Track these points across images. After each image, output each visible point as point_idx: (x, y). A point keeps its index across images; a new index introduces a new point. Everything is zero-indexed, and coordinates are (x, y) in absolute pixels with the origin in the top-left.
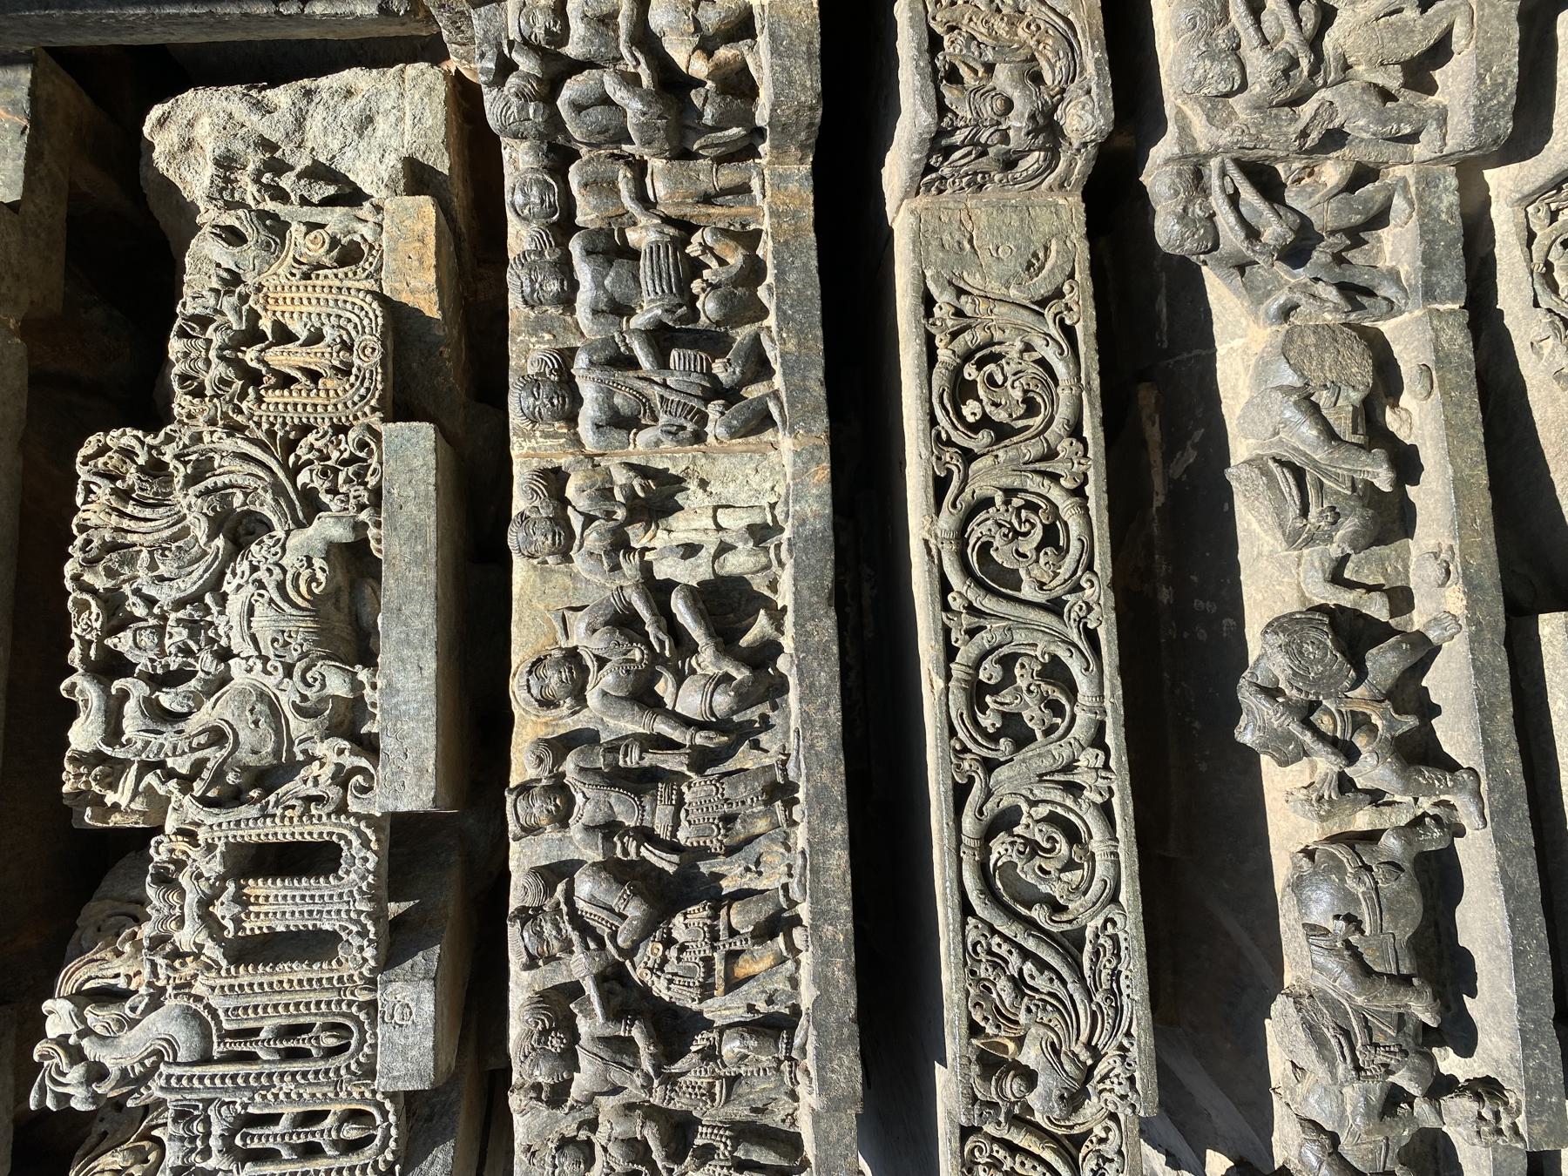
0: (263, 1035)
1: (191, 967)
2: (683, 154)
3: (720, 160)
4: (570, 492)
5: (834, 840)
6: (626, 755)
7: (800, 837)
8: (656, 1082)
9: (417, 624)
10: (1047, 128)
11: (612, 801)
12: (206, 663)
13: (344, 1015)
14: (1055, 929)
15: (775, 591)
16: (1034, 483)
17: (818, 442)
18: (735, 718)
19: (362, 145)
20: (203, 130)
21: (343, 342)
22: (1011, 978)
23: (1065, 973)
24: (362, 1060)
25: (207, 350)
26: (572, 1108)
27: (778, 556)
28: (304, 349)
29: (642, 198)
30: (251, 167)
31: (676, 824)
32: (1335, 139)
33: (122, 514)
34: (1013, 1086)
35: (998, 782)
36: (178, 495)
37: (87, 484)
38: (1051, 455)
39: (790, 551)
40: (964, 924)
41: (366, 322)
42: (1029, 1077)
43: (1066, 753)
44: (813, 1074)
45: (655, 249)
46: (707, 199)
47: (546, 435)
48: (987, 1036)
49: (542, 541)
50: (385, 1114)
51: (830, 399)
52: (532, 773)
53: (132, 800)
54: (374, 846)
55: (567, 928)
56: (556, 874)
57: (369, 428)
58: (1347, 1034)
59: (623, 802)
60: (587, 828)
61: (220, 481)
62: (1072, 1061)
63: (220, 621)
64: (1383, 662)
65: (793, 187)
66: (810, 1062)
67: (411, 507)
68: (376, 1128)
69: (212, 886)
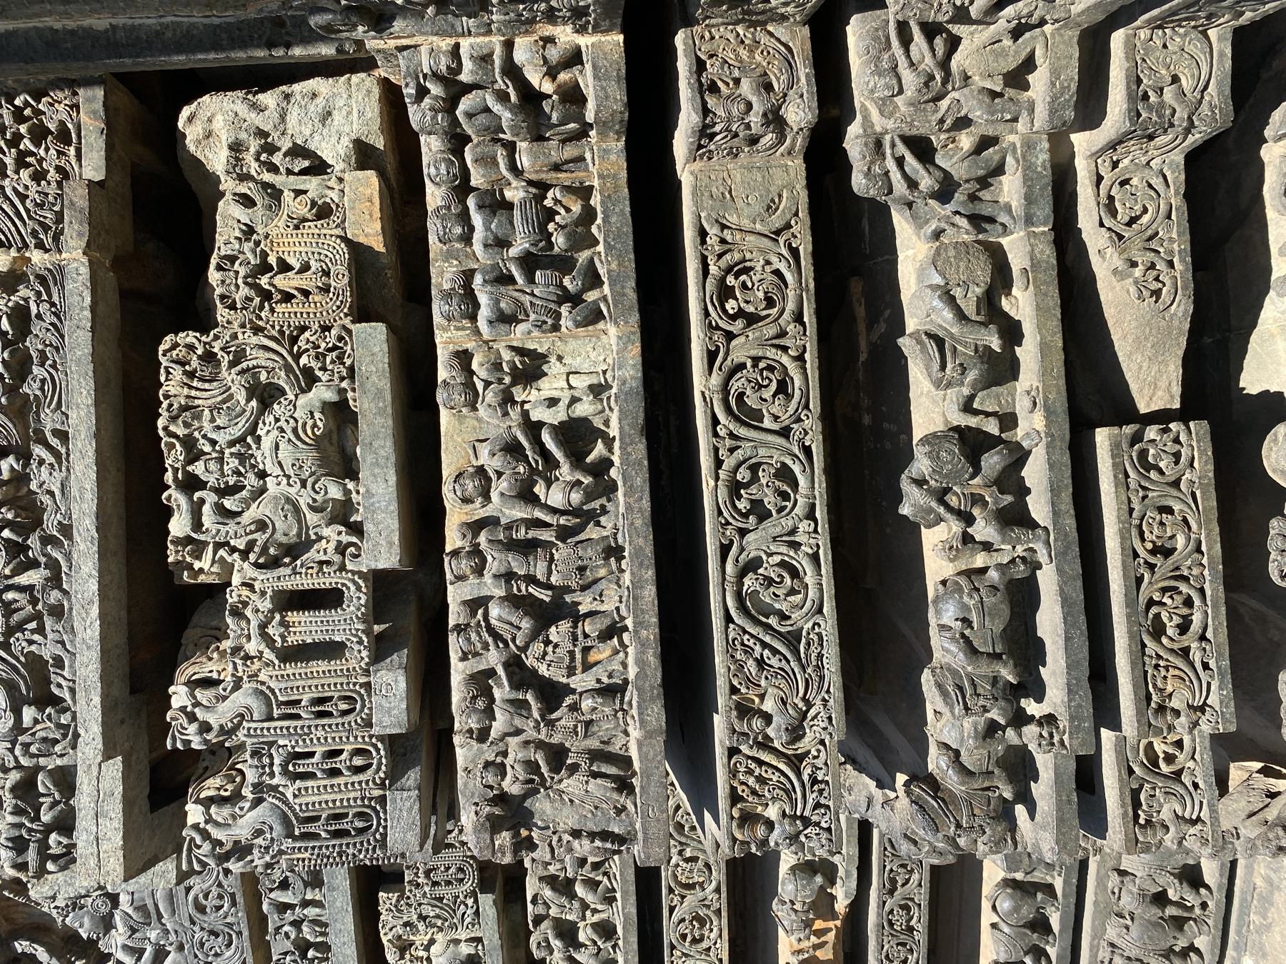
0: (303, 703)
2: (539, 138)
3: (564, 142)
4: (475, 366)
5: (647, 580)
6: (517, 532)
7: (627, 579)
8: (542, 725)
9: (382, 453)
10: (775, 120)
11: (510, 559)
12: (251, 480)
13: (351, 691)
14: (782, 630)
15: (608, 427)
16: (771, 353)
17: (632, 329)
18: (584, 507)
19: (325, 131)
20: (219, 124)
21: (323, 270)
22: (756, 660)
23: (789, 656)
24: (364, 716)
25: (236, 279)
26: (492, 743)
27: (609, 404)
28: (299, 276)
30: (252, 150)
31: (550, 573)
32: (963, 123)
33: (190, 387)
34: (757, 723)
35: (748, 543)
36: (224, 373)
37: (166, 368)
38: (783, 334)
39: (616, 401)
40: (727, 628)
41: (337, 257)
42: (768, 718)
43: (790, 523)
44: (636, 718)
45: (523, 203)
46: (557, 168)
47: (457, 329)
48: (742, 694)
49: (459, 398)
50: (378, 750)
51: (640, 301)
52: (459, 544)
53: (212, 566)
54: (364, 590)
55: (485, 635)
57: (344, 327)
58: (961, 689)
59: (517, 560)
60: (495, 576)
61: (251, 364)
62: (794, 708)
63: (258, 454)
64: (992, 462)
65: (613, 157)
66: (634, 712)
67: (374, 378)
68: (373, 759)
69: (266, 616)
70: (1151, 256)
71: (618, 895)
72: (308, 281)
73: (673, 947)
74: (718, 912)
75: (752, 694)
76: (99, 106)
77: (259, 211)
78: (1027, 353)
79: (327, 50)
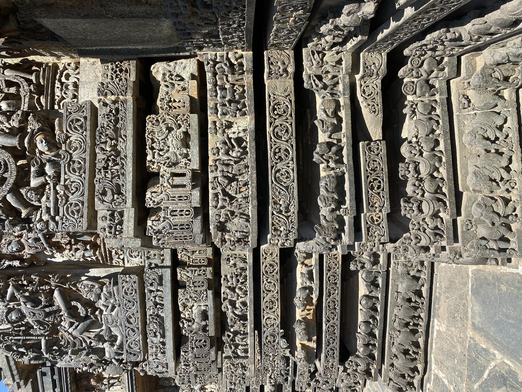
2: (233, 74)
3: (239, 75)
4: (217, 124)
7: (250, 173)
10: (285, 71)
12: (166, 148)
16: (284, 123)
20: (160, 69)
29: (227, 80)
30: (168, 75)
32: (327, 72)
36: (161, 124)
38: (287, 119)
42: (281, 205)
46: (237, 81)
49: (213, 131)
52: (212, 164)
63: (168, 142)
64: (334, 149)
70: (373, 103)
71: (248, 293)
72: (180, 104)
73: (264, 310)
74: (277, 300)
76: (135, 65)
77: (170, 88)
78: (344, 125)
79: (188, 54)
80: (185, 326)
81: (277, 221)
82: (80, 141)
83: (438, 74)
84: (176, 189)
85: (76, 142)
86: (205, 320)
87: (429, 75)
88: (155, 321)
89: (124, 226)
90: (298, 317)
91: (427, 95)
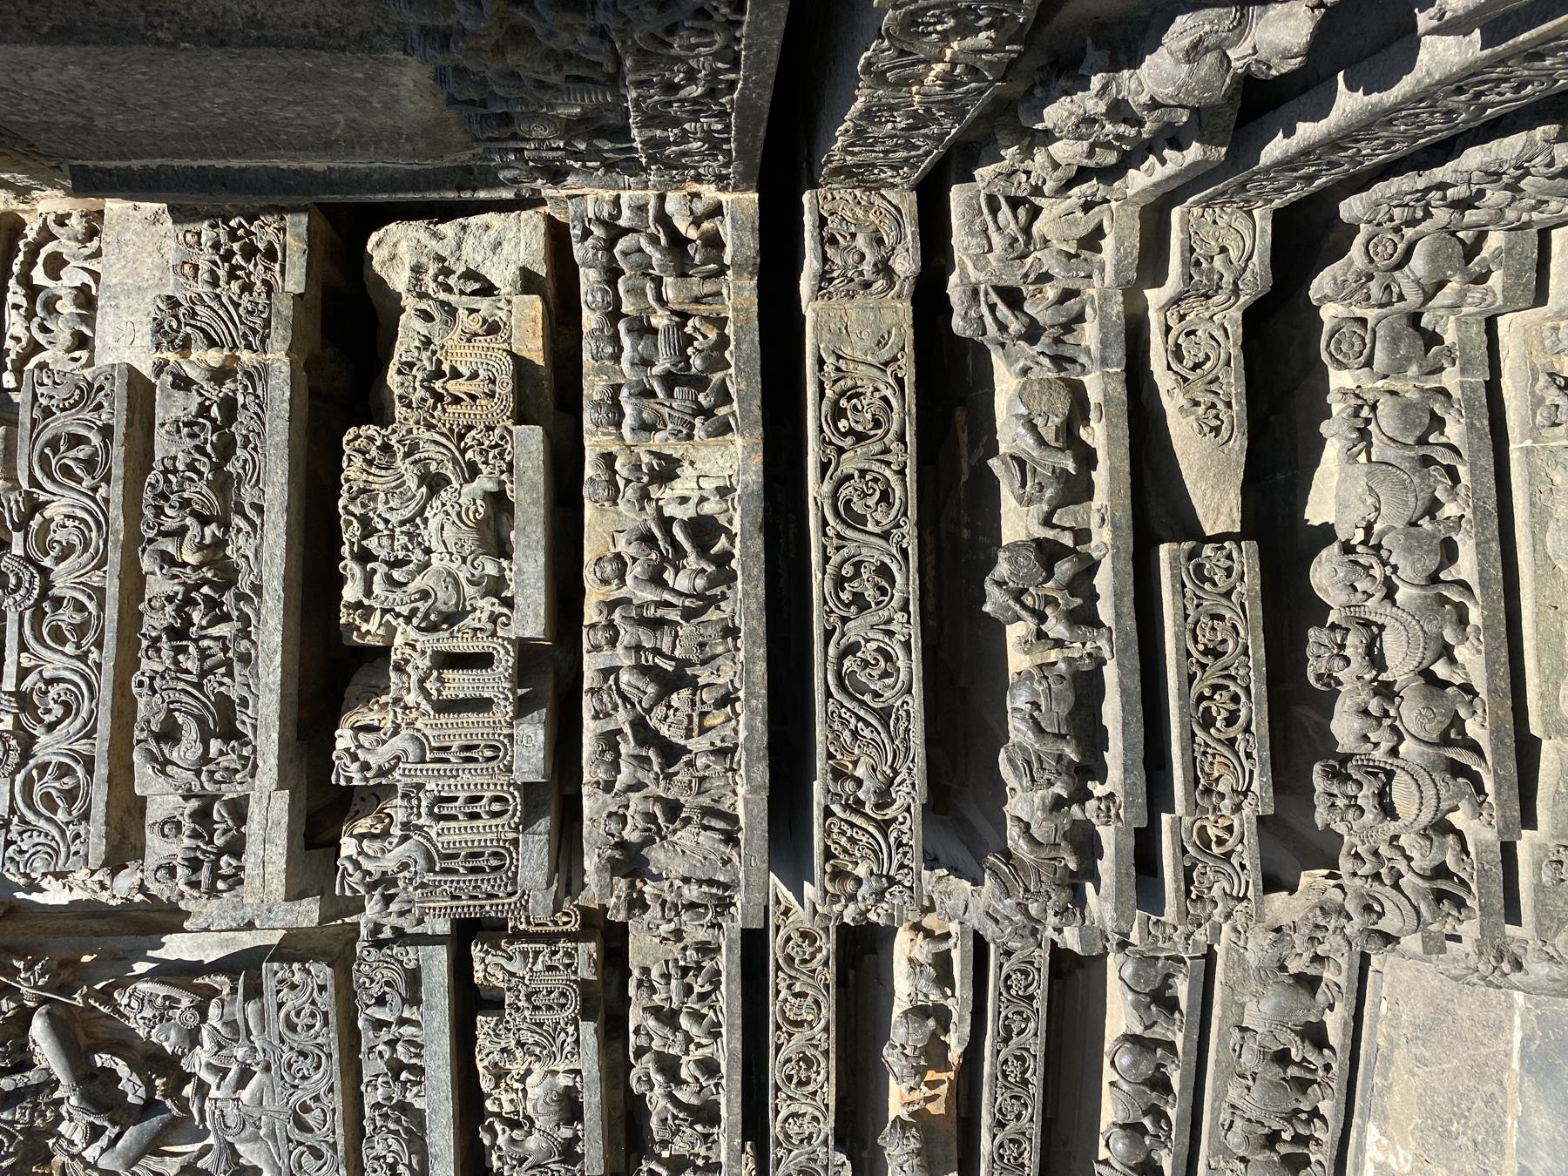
1: (414, 714)
2: (683, 274)
3: (704, 278)
4: (617, 466)
7: (741, 656)
12: (417, 556)
16: (876, 467)
20: (403, 248)
29: (659, 299)
30: (431, 272)
32: (1045, 278)
34: (850, 786)
36: (399, 463)
38: (887, 451)
42: (859, 783)
43: (886, 613)
46: (697, 300)
49: (603, 493)
52: (596, 619)
56: (608, 672)
57: (506, 428)
58: (1029, 763)
63: (425, 534)
64: (1064, 568)
65: (746, 294)
66: (742, 771)
67: (530, 473)
71: (724, 1030)
72: (475, 387)
73: (778, 1089)
74: (826, 1053)
75: (846, 760)
76: (303, 230)
77: (437, 325)
78: (1100, 476)
79: (507, 194)
80: (501, 1141)
81: (843, 841)
82: (83, 521)
83: (1462, 296)
84: (451, 719)
85: (70, 523)
86: (569, 1123)
87: (1429, 297)
88: (392, 1126)
89: (250, 860)
90: (896, 1107)
91: (1413, 370)
